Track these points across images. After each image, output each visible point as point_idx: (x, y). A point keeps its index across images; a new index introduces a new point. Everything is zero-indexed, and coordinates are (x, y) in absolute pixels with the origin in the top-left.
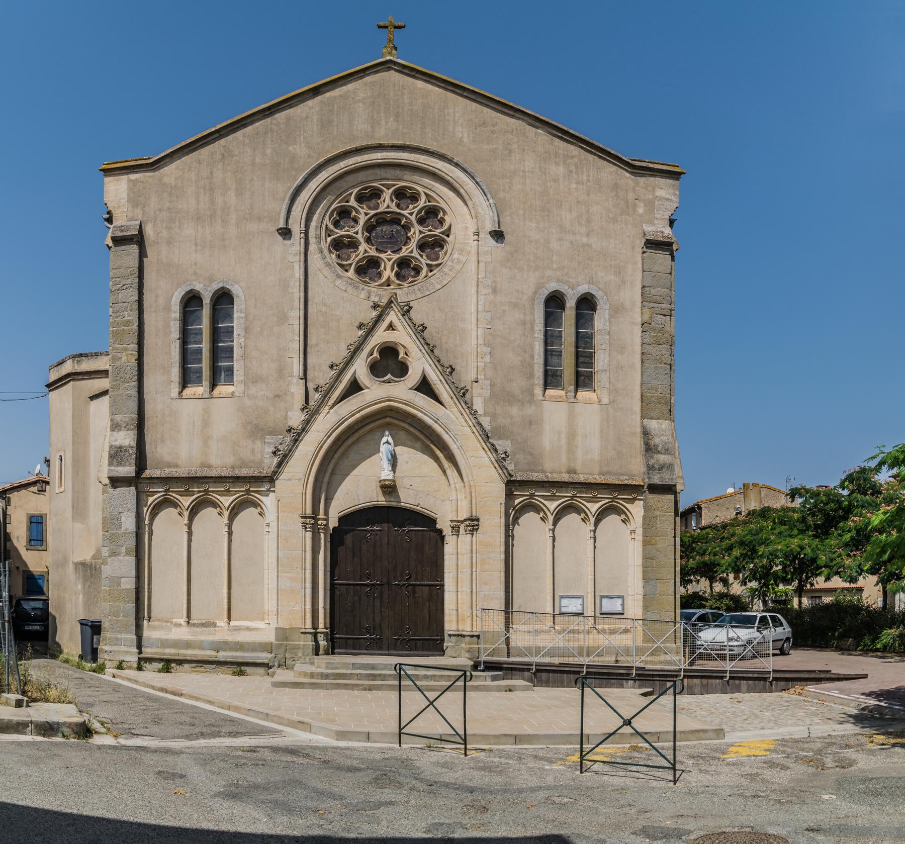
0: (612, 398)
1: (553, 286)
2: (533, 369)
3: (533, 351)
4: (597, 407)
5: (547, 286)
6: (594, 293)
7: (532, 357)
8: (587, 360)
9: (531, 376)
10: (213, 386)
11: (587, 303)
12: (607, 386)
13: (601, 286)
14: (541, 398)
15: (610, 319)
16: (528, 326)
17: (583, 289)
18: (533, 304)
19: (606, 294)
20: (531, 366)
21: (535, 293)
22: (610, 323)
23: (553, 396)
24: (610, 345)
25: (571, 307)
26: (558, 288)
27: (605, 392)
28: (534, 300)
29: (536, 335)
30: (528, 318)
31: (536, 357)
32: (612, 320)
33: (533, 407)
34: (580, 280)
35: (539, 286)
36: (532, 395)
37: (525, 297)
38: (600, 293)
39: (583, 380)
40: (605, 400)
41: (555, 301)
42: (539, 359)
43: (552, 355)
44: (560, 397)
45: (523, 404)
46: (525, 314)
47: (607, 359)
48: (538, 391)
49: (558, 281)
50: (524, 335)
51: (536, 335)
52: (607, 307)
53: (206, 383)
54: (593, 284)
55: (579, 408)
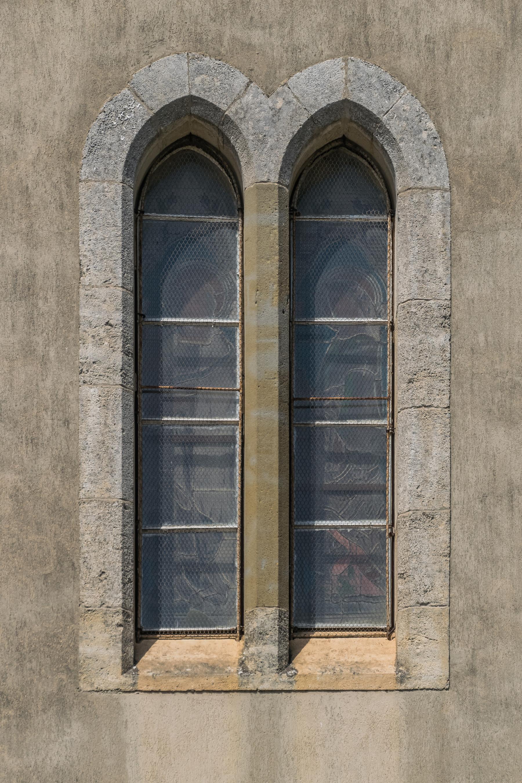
0: (462, 654)
1: (169, 77)
2: (75, 534)
3: (72, 436)
4: (390, 705)
5: (140, 76)
6: (373, 101)
7: (68, 467)
8: (359, 474)
9: (65, 565)
10: (295, 634)
11: (342, 165)
12: (440, 593)
13: (408, 63)
14: (114, 677)
15: (451, 245)
16: (48, 304)
17: (321, 83)
18: (71, 181)
19: (432, 106)
20: (65, 513)
21: (82, 118)
22: (453, 261)
23: (180, 668)
24: (454, 379)
25: (262, 187)
26: (198, 86)
27: (432, 626)
28: (73, 156)
29: (89, 351)
30: (45, 260)
31: (88, 466)
32: (464, 242)
33: (76, 730)
34: (303, 35)
35: (104, 78)
36: (70, 665)
37: (32, 144)
38: (405, 102)
39: (322, 582)
40: (430, 669)
41: (180, 164)
42: (103, 481)
43: (189, 461)
44: (211, 668)
45: (24, 714)
46: (31, 239)
47: (439, 452)
48: (101, 644)
49: (199, 45)
50: (28, 350)
51: (89, 351)
52: (437, 175)
53: (265, 617)
54: (368, 56)
55: (302, 719)
